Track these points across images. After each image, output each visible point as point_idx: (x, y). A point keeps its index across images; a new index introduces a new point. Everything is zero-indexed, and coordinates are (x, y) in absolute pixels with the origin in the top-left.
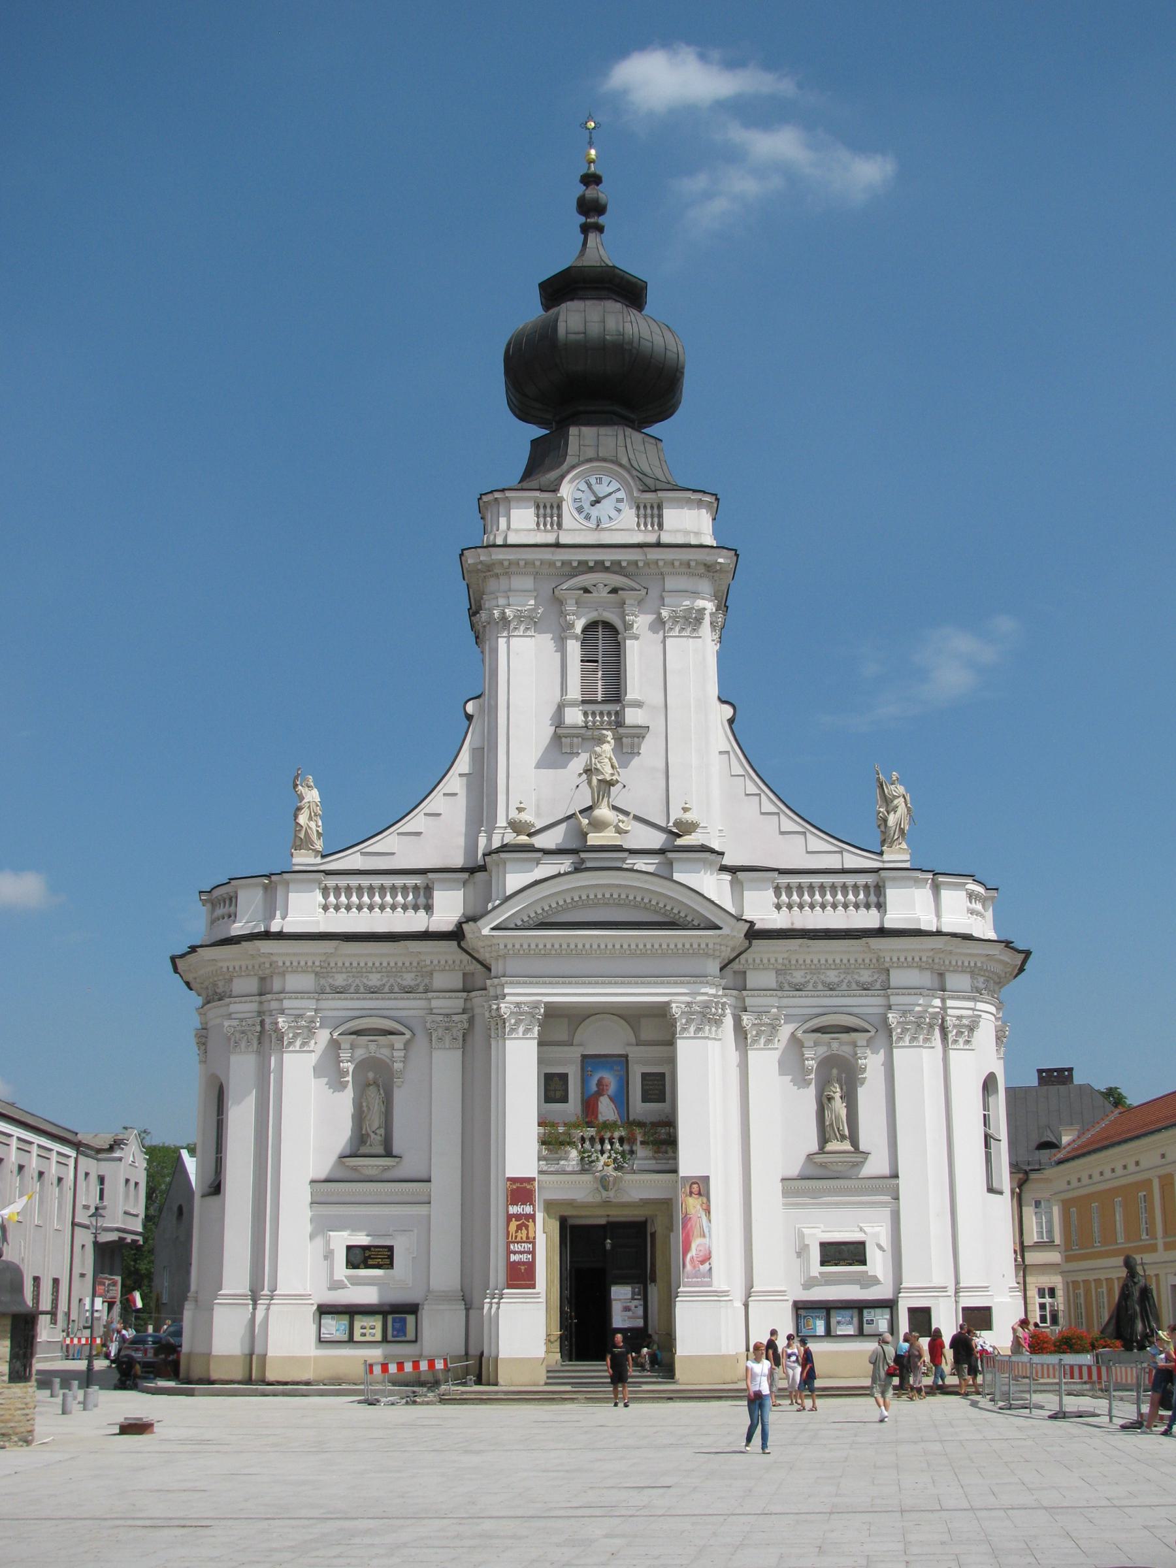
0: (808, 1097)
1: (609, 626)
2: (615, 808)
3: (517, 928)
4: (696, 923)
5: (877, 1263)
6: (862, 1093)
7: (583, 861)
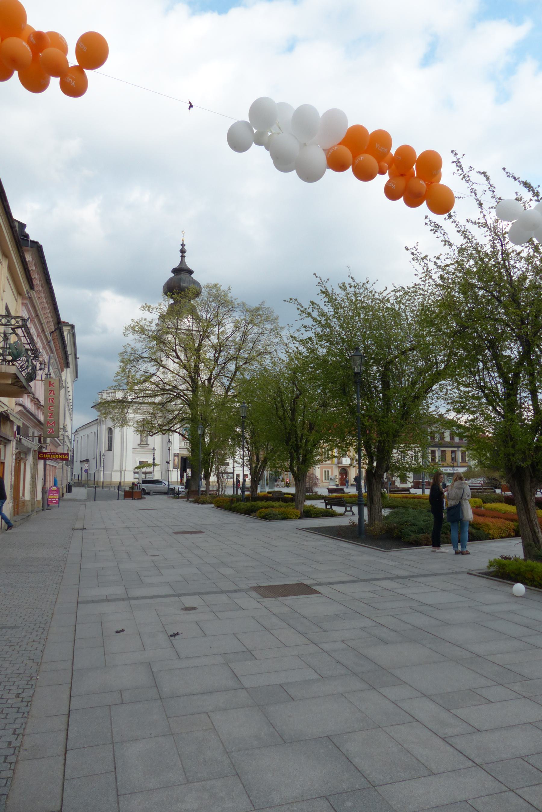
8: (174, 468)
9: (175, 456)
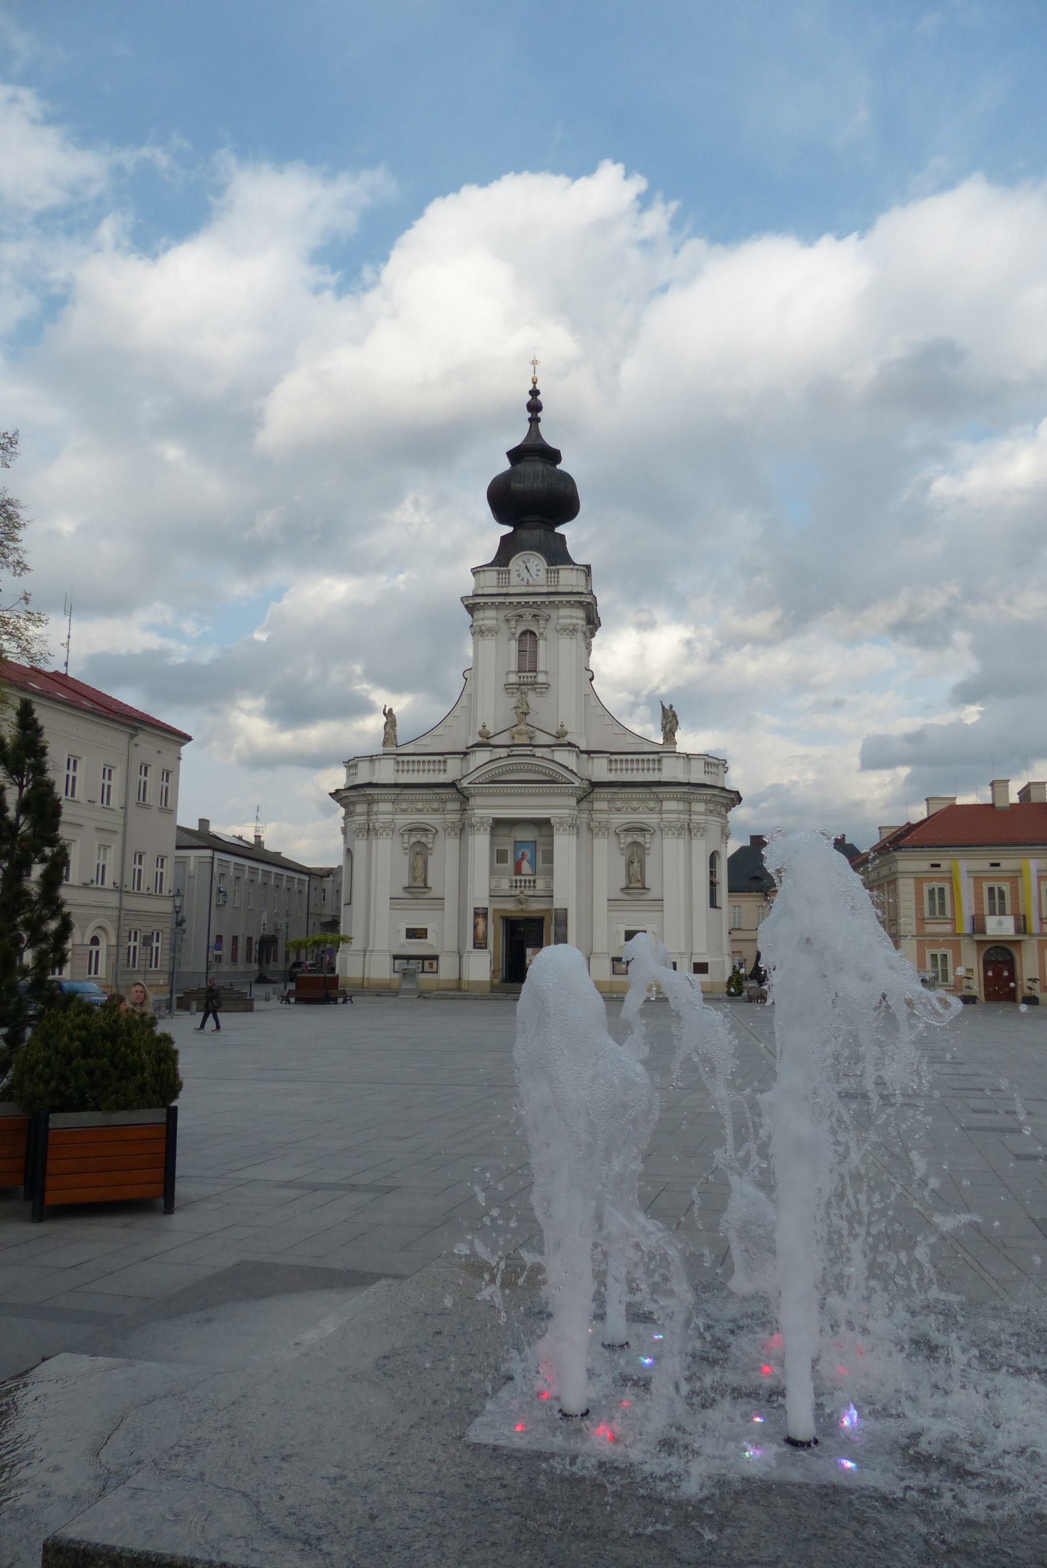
0: (622, 862)
1: (532, 633)
3: (480, 783)
4: (563, 781)
7: (512, 751)
8: (475, 947)
9: (476, 914)
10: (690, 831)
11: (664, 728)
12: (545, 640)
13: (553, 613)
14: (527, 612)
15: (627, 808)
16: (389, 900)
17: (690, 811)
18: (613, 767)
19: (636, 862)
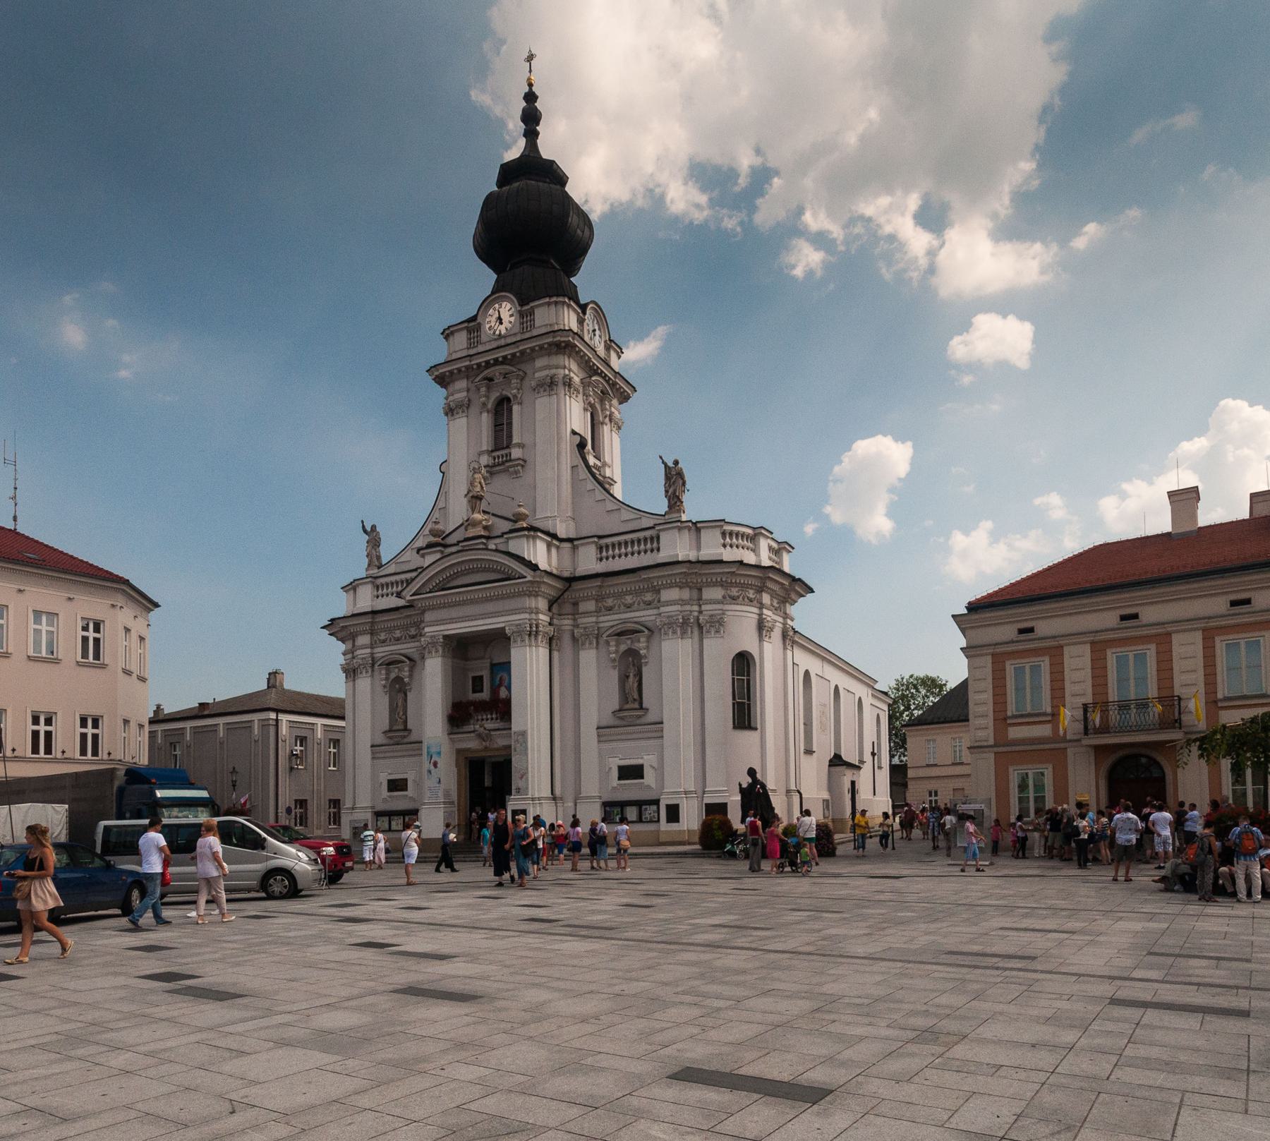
0: (614, 675)
1: (508, 400)
2: (484, 512)
3: (427, 593)
4: (517, 576)
5: (649, 778)
6: (645, 669)
10: (700, 627)
11: (667, 492)
12: (520, 403)
13: (527, 367)
14: (496, 371)
15: (619, 607)
16: (370, 749)
17: (700, 599)
18: (604, 554)
19: (631, 675)
